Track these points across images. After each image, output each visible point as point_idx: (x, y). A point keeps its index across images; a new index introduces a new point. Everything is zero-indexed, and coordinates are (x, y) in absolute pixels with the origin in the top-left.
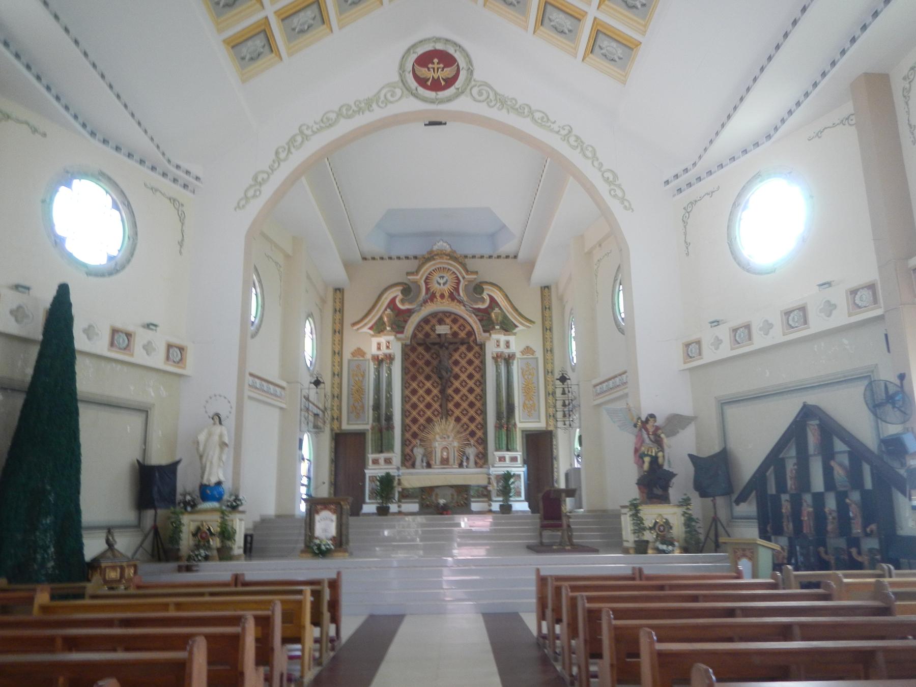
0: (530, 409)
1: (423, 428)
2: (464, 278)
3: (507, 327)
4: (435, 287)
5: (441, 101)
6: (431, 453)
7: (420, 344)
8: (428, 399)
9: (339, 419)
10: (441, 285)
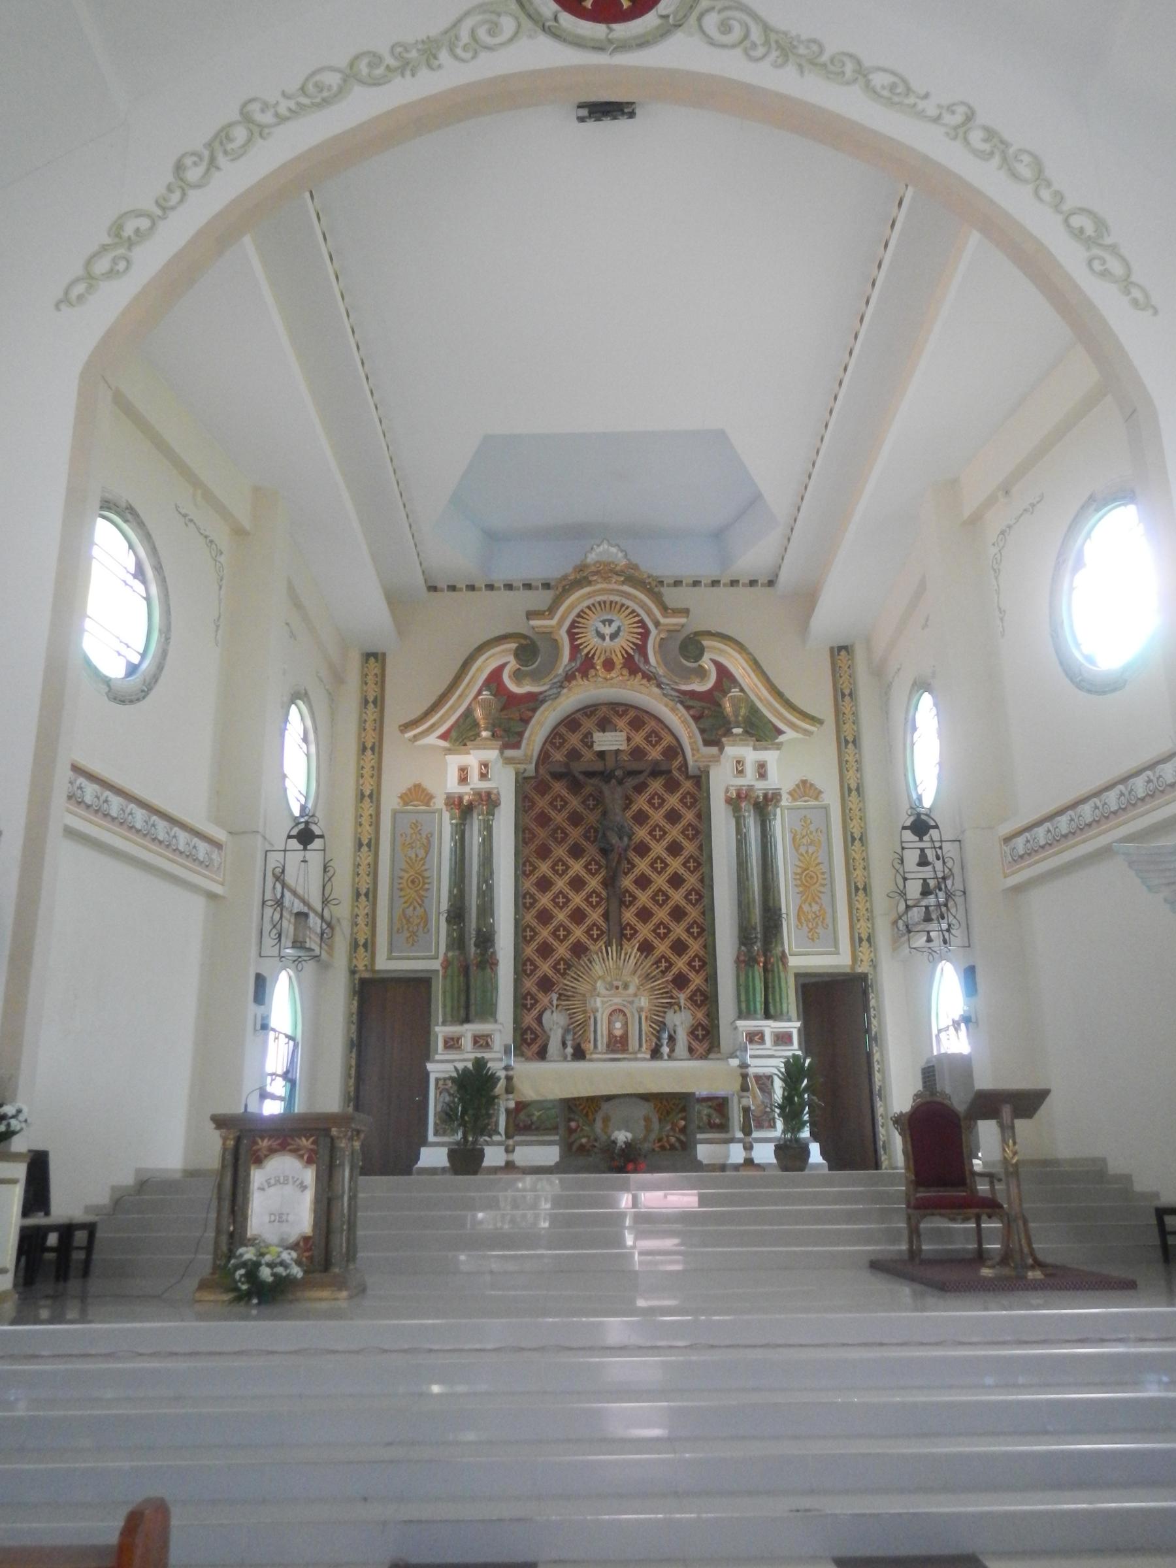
0: (817, 925)
1: (564, 968)
2: (657, 624)
3: (760, 731)
4: (590, 641)
5: (623, 46)
6: (584, 1024)
7: (557, 776)
8: (577, 900)
9: (370, 946)
10: (607, 637)
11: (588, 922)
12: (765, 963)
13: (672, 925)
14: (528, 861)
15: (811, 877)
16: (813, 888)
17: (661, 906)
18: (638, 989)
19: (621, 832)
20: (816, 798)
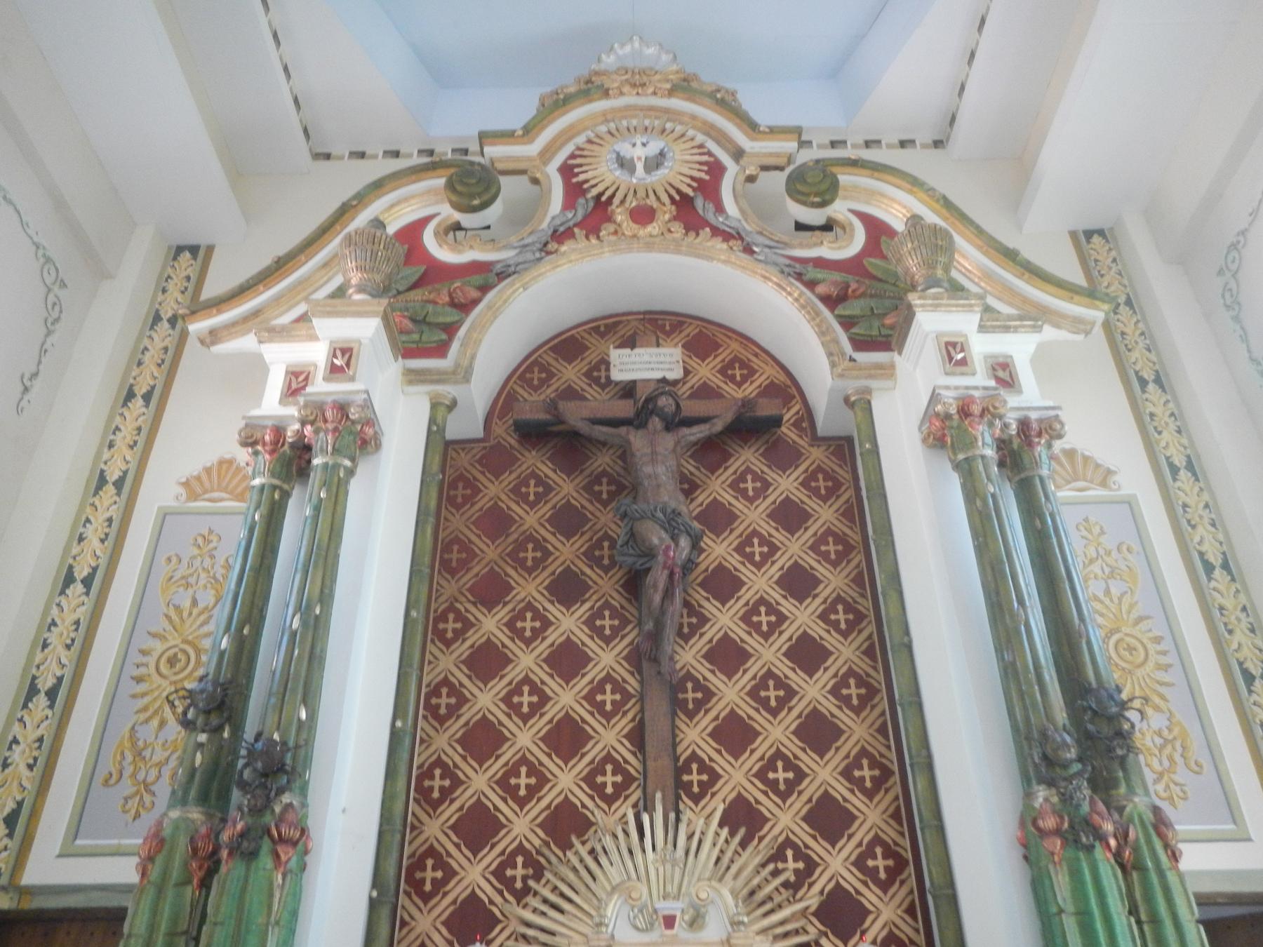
1: (523, 875)
2: (738, 154)
4: (602, 173)
7: (532, 434)
8: (566, 698)
11: (593, 752)
13: (807, 760)
14: (451, 608)
15: (1131, 649)
16: (1140, 673)
17: (774, 712)
18: (735, 924)
19: (672, 524)
20: (1104, 484)
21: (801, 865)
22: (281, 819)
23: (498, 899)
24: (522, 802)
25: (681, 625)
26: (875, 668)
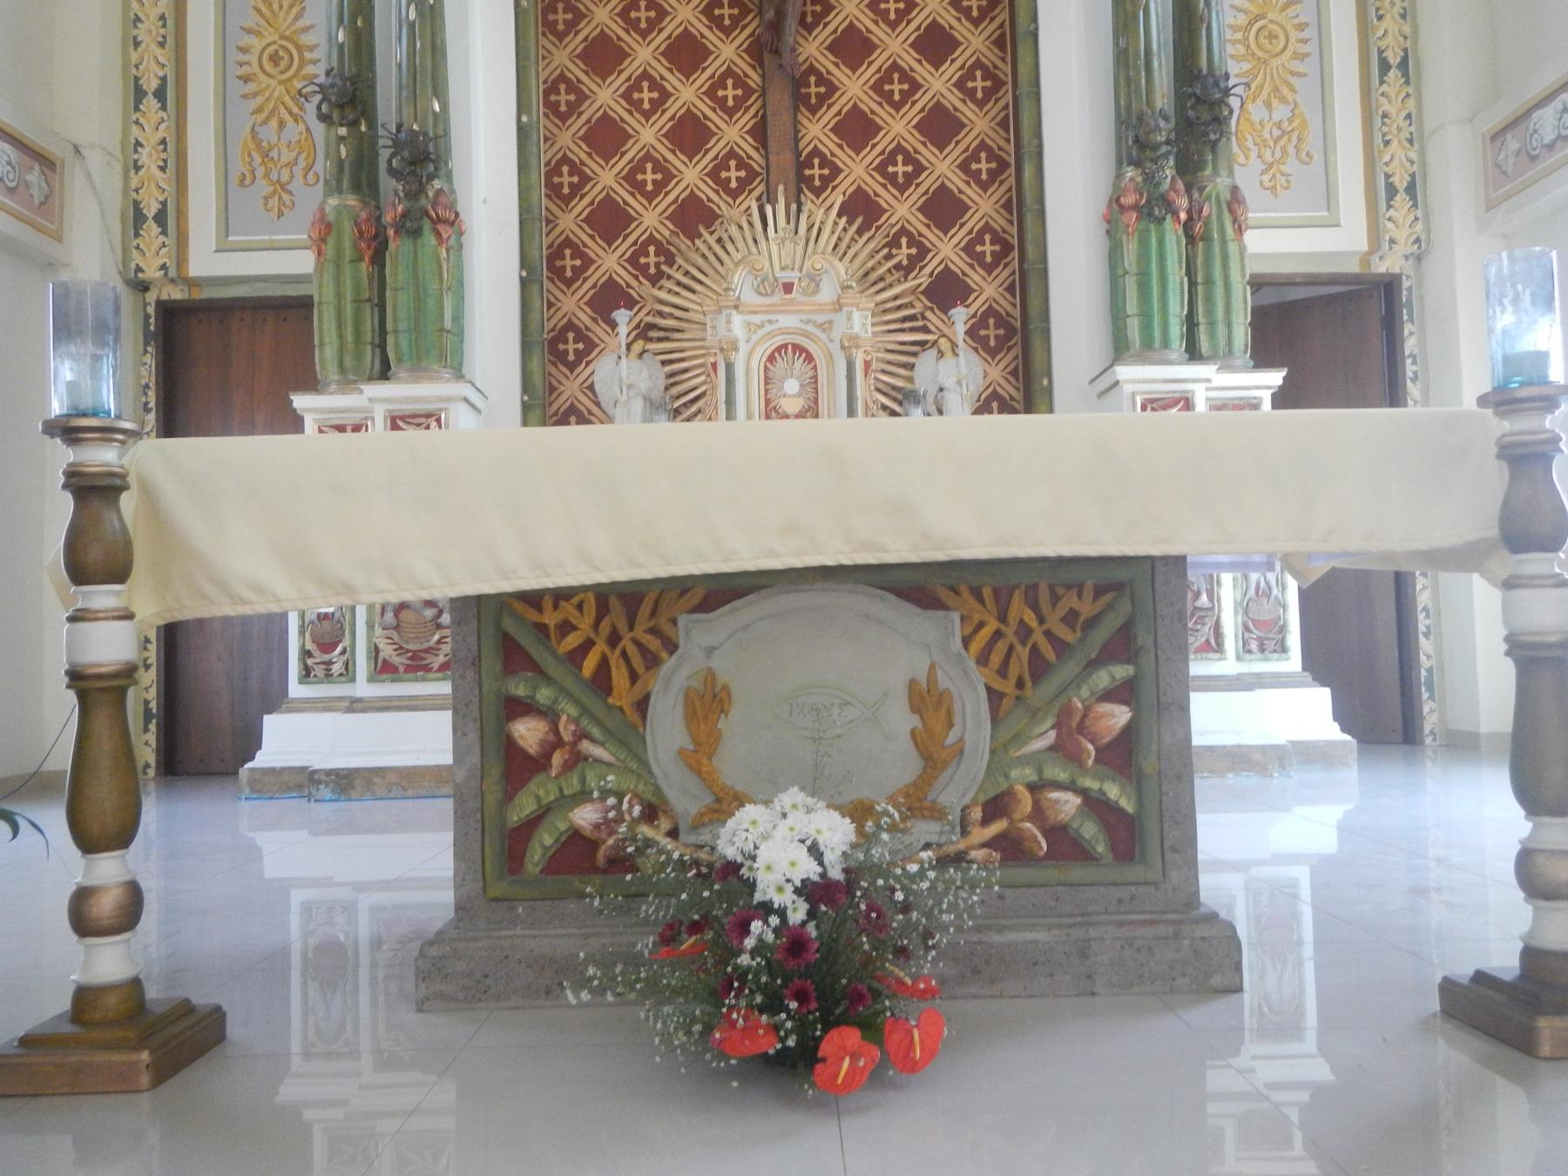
1: (653, 262)
8: (687, 94)
9: (171, 218)
12: (1189, 212)
13: (927, 154)
15: (1272, 37)
16: (1275, 62)
17: (897, 106)
18: (845, 288)
21: (914, 251)
22: (435, 203)
23: (634, 283)
24: (650, 197)
25: (804, 14)
26: (1003, 59)
